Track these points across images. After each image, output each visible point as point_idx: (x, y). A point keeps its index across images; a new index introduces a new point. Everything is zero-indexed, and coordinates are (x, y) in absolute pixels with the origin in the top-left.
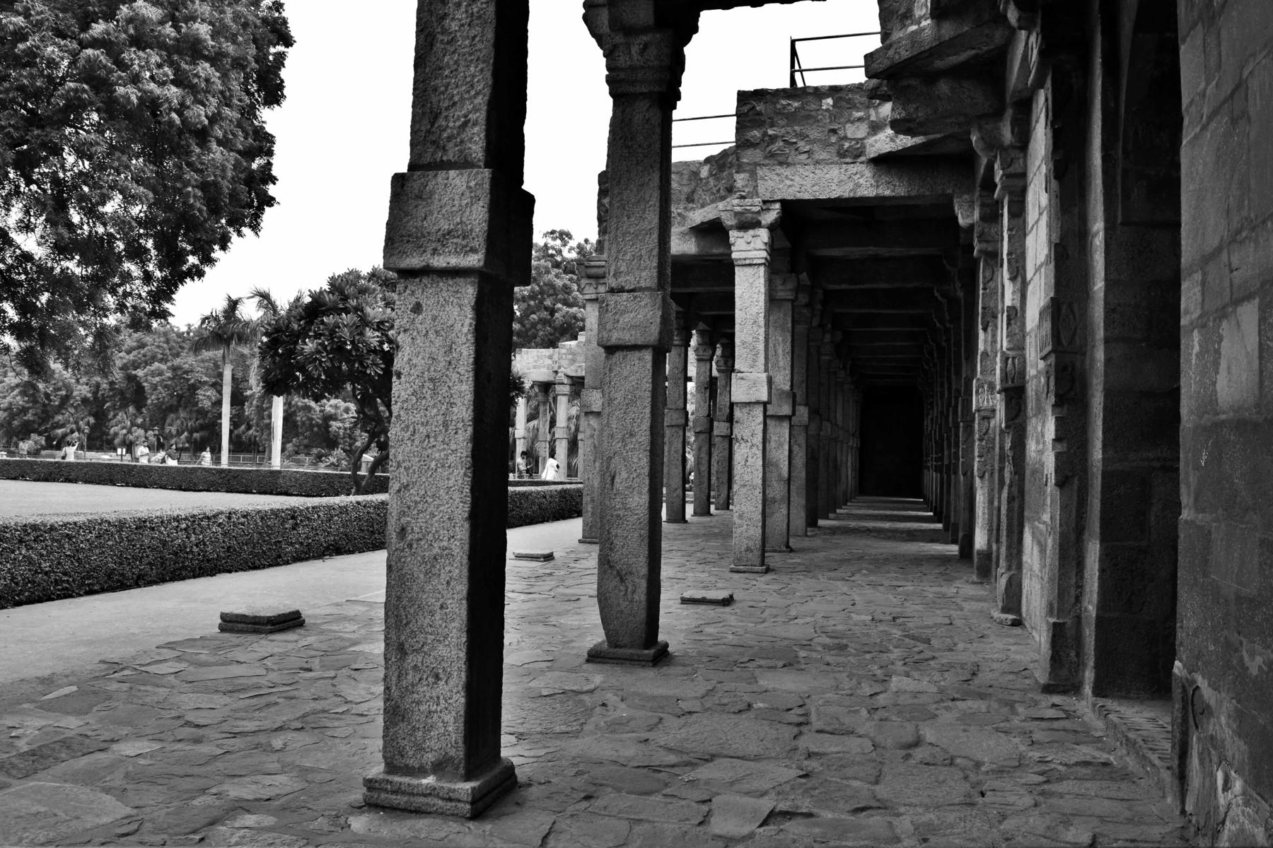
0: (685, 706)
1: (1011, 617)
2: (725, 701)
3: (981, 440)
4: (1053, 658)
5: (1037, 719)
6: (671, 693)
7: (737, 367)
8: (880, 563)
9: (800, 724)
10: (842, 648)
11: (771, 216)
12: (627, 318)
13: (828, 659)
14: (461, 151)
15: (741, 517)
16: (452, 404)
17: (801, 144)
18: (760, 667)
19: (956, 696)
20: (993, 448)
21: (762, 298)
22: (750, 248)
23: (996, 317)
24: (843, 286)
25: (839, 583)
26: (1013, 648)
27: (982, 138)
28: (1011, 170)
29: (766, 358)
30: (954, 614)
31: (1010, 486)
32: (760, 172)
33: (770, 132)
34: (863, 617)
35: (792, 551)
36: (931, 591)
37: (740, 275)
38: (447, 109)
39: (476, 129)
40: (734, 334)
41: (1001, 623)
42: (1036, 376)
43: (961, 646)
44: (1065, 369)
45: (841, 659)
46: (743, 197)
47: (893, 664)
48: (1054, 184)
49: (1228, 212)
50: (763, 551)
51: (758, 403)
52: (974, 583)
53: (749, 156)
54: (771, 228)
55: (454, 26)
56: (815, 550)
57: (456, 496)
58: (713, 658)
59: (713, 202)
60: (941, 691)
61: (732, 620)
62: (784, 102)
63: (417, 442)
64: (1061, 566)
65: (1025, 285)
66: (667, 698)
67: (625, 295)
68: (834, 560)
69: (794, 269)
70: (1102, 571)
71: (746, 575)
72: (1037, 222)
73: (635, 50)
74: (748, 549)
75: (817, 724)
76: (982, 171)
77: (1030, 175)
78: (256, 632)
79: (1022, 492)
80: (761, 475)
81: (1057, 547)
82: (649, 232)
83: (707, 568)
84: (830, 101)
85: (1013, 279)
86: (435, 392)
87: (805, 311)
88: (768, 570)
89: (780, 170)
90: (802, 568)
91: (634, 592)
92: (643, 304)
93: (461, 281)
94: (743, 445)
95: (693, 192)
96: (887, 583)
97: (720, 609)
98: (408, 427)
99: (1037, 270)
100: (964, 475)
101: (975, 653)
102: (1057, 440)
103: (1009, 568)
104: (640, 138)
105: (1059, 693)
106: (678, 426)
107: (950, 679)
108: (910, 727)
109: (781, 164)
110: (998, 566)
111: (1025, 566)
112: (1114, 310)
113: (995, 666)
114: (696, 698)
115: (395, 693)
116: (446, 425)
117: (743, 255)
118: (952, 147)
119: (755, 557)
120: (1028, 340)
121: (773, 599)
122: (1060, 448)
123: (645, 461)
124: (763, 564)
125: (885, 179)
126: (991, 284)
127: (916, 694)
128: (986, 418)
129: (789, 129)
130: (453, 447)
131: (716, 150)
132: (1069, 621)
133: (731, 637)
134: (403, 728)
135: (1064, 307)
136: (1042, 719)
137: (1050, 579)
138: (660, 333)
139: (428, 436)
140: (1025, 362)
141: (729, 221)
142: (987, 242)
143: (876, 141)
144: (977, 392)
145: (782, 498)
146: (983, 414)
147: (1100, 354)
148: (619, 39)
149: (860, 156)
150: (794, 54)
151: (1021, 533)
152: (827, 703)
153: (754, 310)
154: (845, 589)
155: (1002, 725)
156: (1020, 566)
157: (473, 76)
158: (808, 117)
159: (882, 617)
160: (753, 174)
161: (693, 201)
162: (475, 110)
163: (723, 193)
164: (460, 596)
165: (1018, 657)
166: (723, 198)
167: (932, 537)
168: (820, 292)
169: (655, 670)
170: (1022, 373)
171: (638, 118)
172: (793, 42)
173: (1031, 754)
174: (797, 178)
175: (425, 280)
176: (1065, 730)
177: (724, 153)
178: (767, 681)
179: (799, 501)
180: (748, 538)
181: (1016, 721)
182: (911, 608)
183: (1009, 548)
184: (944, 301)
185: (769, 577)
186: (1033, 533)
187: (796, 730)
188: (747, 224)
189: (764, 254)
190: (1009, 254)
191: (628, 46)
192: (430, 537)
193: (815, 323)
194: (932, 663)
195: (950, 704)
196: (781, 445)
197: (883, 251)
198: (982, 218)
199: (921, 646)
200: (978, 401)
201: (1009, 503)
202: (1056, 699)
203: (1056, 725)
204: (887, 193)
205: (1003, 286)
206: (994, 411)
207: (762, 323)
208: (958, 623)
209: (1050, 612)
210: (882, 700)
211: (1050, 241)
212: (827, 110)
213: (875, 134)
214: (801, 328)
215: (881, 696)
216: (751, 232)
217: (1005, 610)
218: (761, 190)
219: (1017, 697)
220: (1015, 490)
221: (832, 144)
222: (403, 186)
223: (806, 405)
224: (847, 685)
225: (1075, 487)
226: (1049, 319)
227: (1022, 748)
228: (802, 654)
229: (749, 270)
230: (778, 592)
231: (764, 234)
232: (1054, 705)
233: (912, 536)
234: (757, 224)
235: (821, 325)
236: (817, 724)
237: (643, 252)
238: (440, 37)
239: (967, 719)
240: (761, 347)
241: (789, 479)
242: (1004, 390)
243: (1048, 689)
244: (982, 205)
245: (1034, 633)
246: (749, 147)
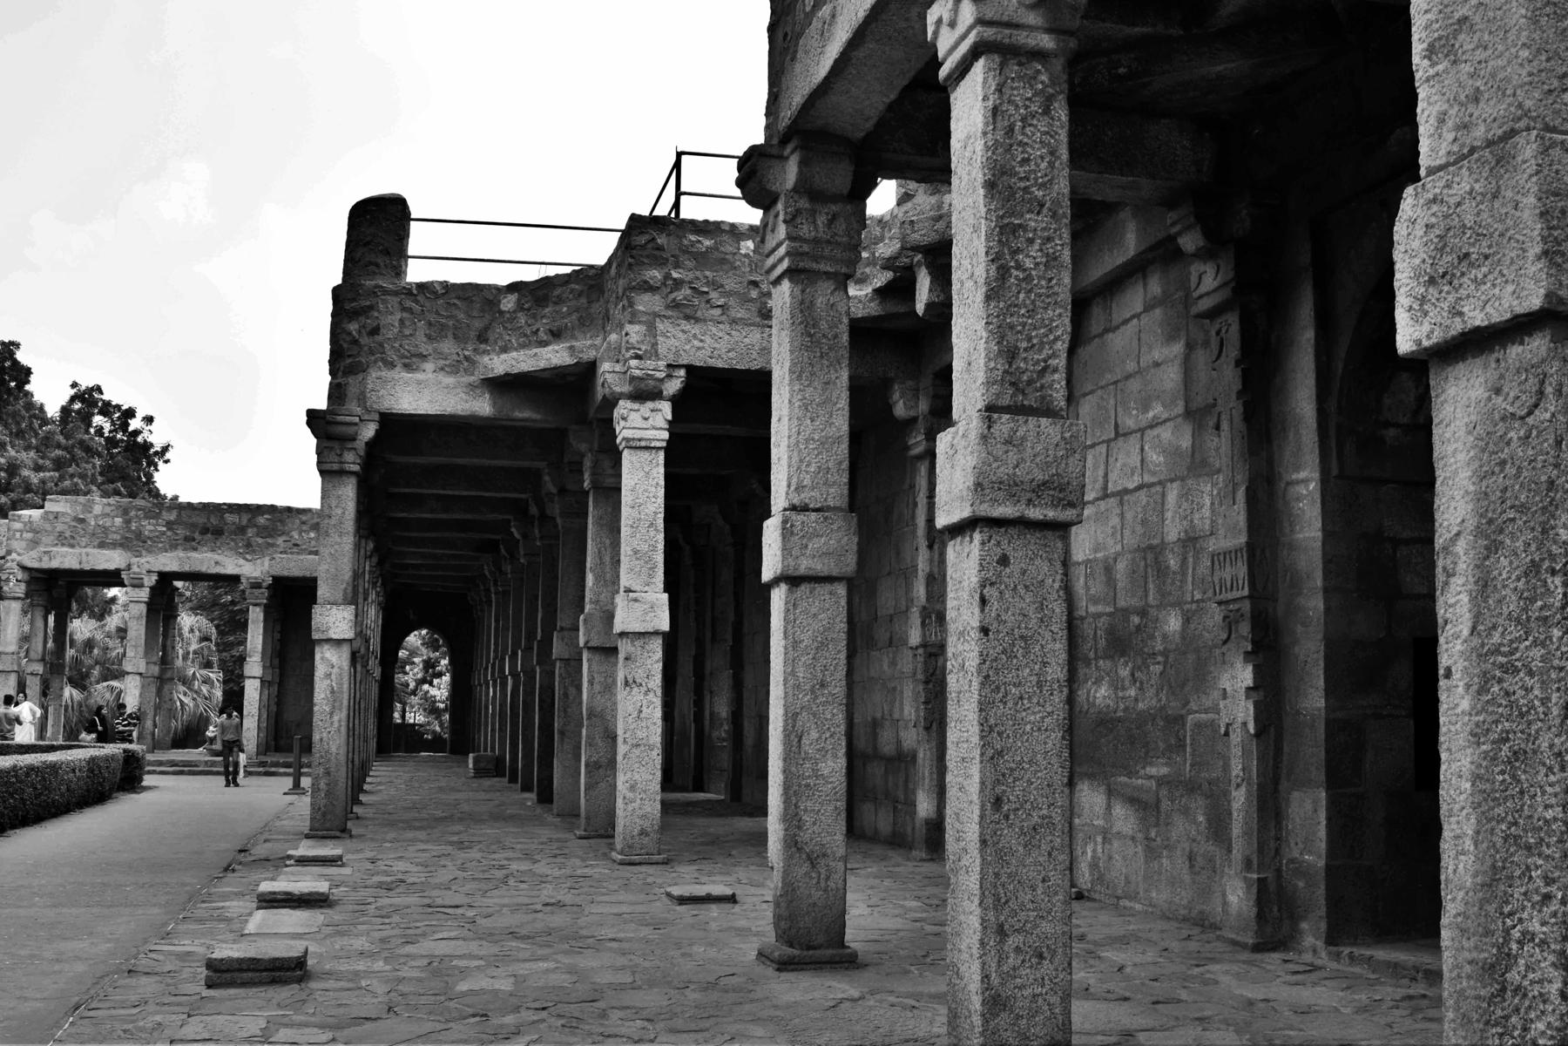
11: (673, 386)
12: (815, 544)
14: (1043, 398)
16: (1045, 664)
17: (713, 295)
32: (660, 326)
33: (675, 275)
38: (1025, 350)
39: (1056, 376)
51: (656, 633)
52: (922, 860)
54: (677, 402)
55: (1029, 264)
57: (1054, 760)
59: (523, 346)
62: (693, 238)
63: (1010, 704)
64: (1260, 818)
67: (813, 516)
70: (1329, 819)
71: (643, 869)
73: (821, 220)
74: (643, 833)
78: (273, 982)
82: (838, 440)
84: (750, 244)
86: (1027, 653)
91: (828, 878)
92: (835, 527)
93: (1049, 534)
95: (487, 328)
98: (998, 688)
104: (824, 325)
109: (687, 318)
112: (1330, 561)
115: (995, 980)
116: (1040, 685)
122: (1259, 695)
123: (840, 718)
129: (698, 273)
130: (1049, 709)
131: (531, 274)
132: (1269, 875)
134: (1004, 1019)
135: (1258, 553)
139: (1021, 698)
146: (930, 650)
147: (1314, 604)
148: (804, 203)
150: (677, 166)
153: (651, 508)
157: (1052, 320)
158: (723, 261)
160: (651, 328)
161: (486, 341)
162: (1054, 355)
163: (542, 335)
164: (1062, 867)
171: (820, 301)
172: (679, 155)
174: (708, 339)
175: (1012, 531)
177: (546, 282)
180: (644, 817)
188: (644, 393)
189: (666, 435)
191: (813, 213)
192: (1028, 806)
212: (747, 256)
216: (650, 405)
218: (662, 350)
221: (752, 300)
222: (989, 427)
229: (646, 455)
231: (666, 409)
234: (656, 395)
237: (830, 465)
238: (1015, 273)
246: (646, 290)
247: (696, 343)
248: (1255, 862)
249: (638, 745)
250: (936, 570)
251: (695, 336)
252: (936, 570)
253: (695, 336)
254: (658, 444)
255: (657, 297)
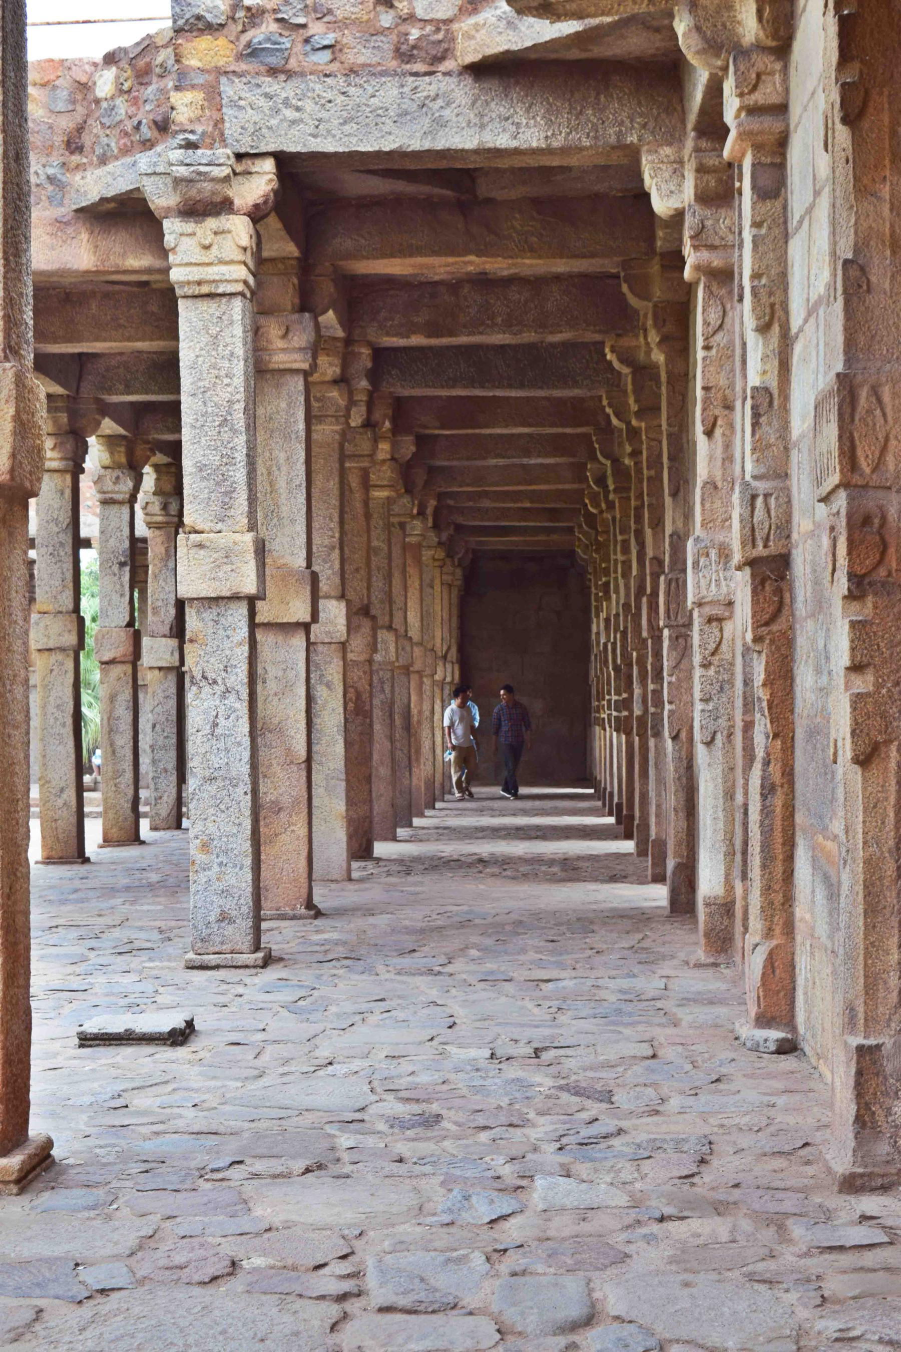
0: (93, 1277)
1: (775, 1035)
2: (179, 1259)
3: (705, 666)
4: (859, 1119)
5: (831, 1248)
6: (59, 1250)
7: (188, 519)
8: (506, 931)
9: (342, 1298)
10: (432, 1121)
13: (402, 1148)
15: (205, 847)
17: (316, 29)
18: (256, 1176)
19: (668, 1211)
20: (732, 684)
21: (239, 368)
22: (211, 257)
23: (729, 407)
24: (417, 340)
25: (422, 982)
26: (781, 1101)
27: (698, 29)
28: (758, 98)
29: (252, 500)
30: (662, 1034)
31: (767, 763)
32: (229, 89)
34: (473, 1053)
35: (319, 914)
36: (612, 988)
37: (189, 316)
40: (178, 445)
41: (756, 1048)
42: (812, 534)
43: (675, 1103)
44: (867, 520)
45: (426, 1148)
46: (191, 145)
47: (535, 1149)
48: (843, 134)
49: (600, 1236)
50: (258, 919)
51: (235, 598)
52: (698, 965)
53: (202, 52)
54: (256, 215)
56: (369, 911)
58: (151, 1165)
59: (125, 151)
60: (636, 1204)
61: (193, 1076)
65: (786, 342)
66: (50, 1261)
68: (409, 931)
69: (306, 304)
72: (810, 210)
74: (224, 917)
75: (379, 1292)
76: (697, 96)
77: (795, 110)
79: (789, 773)
80: (246, 755)
81: (860, 888)
83: (135, 962)
85: (763, 329)
87: (335, 394)
88: (268, 961)
89: (271, 85)
90: (341, 951)
94: (207, 689)
95: (80, 129)
96: (521, 975)
97: (167, 1053)
99: (811, 312)
100: (675, 738)
101: (704, 1116)
102: (856, 668)
103: (769, 933)
105: (873, 1190)
106: (62, 649)
107: (659, 1175)
108: (573, 1285)
109: (273, 72)
110: (746, 929)
111: (800, 926)
113: (745, 1141)
114: (116, 1257)
117: (195, 274)
118: (636, 44)
119: (239, 933)
120: (794, 455)
121: (284, 1025)
122: (864, 683)
124: (257, 948)
125: (498, 108)
126: (719, 339)
127: (585, 1213)
128: (720, 620)
131: (128, 37)
133: (190, 1113)
135: (864, 393)
136: (841, 1248)
137: (849, 957)
138: (13, 456)
140: (789, 502)
141: (161, 198)
142: (712, 247)
143: (477, 27)
144: (696, 564)
145: (296, 802)
146: (708, 610)
149: (441, 59)
151: (790, 858)
152: (401, 1246)
153: (224, 395)
154: (434, 994)
155: (760, 1267)
156: (789, 928)
159: (512, 1051)
160: (213, 94)
161: (80, 149)
163: (147, 132)
165: (791, 1120)
166: (148, 145)
167: (612, 871)
168: (365, 351)
169: (25, 1199)
170: (784, 528)
173: (820, 1325)
174: (308, 105)
176: (887, 1269)
177: (148, 46)
178: (270, 1207)
179: (333, 806)
181: (788, 1257)
182: (570, 1027)
183: (767, 889)
184: (626, 370)
185: (272, 974)
186: (814, 859)
187: (333, 1310)
189: (242, 272)
190: (756, 276)
193: (356, 420)
194: (616, 1142)
195: (655, 1228)
196: (288, 687)
197: (498, 266)
198: (703, 198)
199: (594, 1108)
200: (698, 585)
201: (764, 797)
202: (870, 1204)
203: (869, 1258)
204: (503, 141)
205: (744, 345)
206: (730, 604)
207: (239, 419)
208: (668, 1053)
209: (851, 1023)
210: (513, 1231)
211: (834, 254)
213: (475, 11)
214: (326, 431)
215: (512, 1221)
216: (212, 223)
217: (764, 1020)
218: (231, 129)
219: (789, 1204)
220: (775, 770)
221: (383, 32)
223: (342, 596)
224: (441, 1201)
225: (893, 765)
226: (834, 417)
227: (803, 1313)
228: (345, 1140)
229: (211, 308)
230: (291, 1007)
231: (240, 229)
232: (865, 1218)
233: (571, 870)
234: (224, 206)
235: (369, 424)
236: (379, 1294)
239: (689, 1261)
240: (240, 475)
241: (309, 760)
242: (752, 563)
243: (852, 1185)
244: (701, 170)
245: (823, 1068)
247: (290, 114)
248: (861, 1010)
249: (212, 779)
250: (718, 475)
251: (286, 102)
252: (718, 475)
253: (286, 102)
254: (230, 288)
255: (222, 41)
